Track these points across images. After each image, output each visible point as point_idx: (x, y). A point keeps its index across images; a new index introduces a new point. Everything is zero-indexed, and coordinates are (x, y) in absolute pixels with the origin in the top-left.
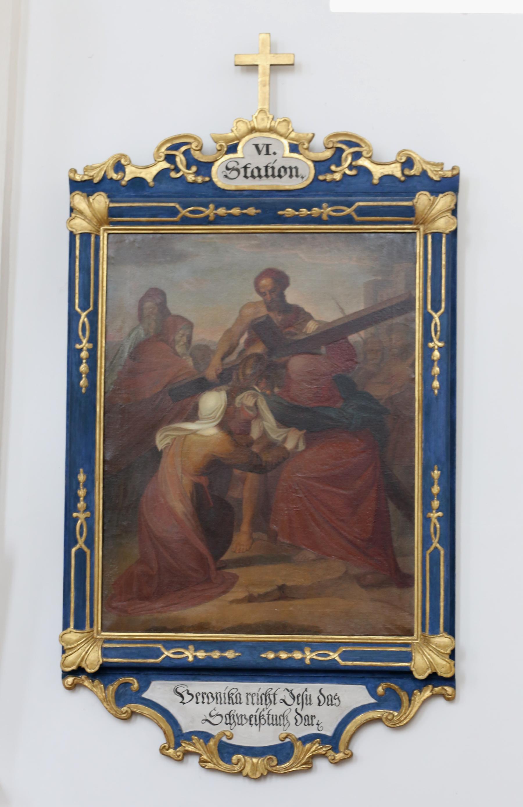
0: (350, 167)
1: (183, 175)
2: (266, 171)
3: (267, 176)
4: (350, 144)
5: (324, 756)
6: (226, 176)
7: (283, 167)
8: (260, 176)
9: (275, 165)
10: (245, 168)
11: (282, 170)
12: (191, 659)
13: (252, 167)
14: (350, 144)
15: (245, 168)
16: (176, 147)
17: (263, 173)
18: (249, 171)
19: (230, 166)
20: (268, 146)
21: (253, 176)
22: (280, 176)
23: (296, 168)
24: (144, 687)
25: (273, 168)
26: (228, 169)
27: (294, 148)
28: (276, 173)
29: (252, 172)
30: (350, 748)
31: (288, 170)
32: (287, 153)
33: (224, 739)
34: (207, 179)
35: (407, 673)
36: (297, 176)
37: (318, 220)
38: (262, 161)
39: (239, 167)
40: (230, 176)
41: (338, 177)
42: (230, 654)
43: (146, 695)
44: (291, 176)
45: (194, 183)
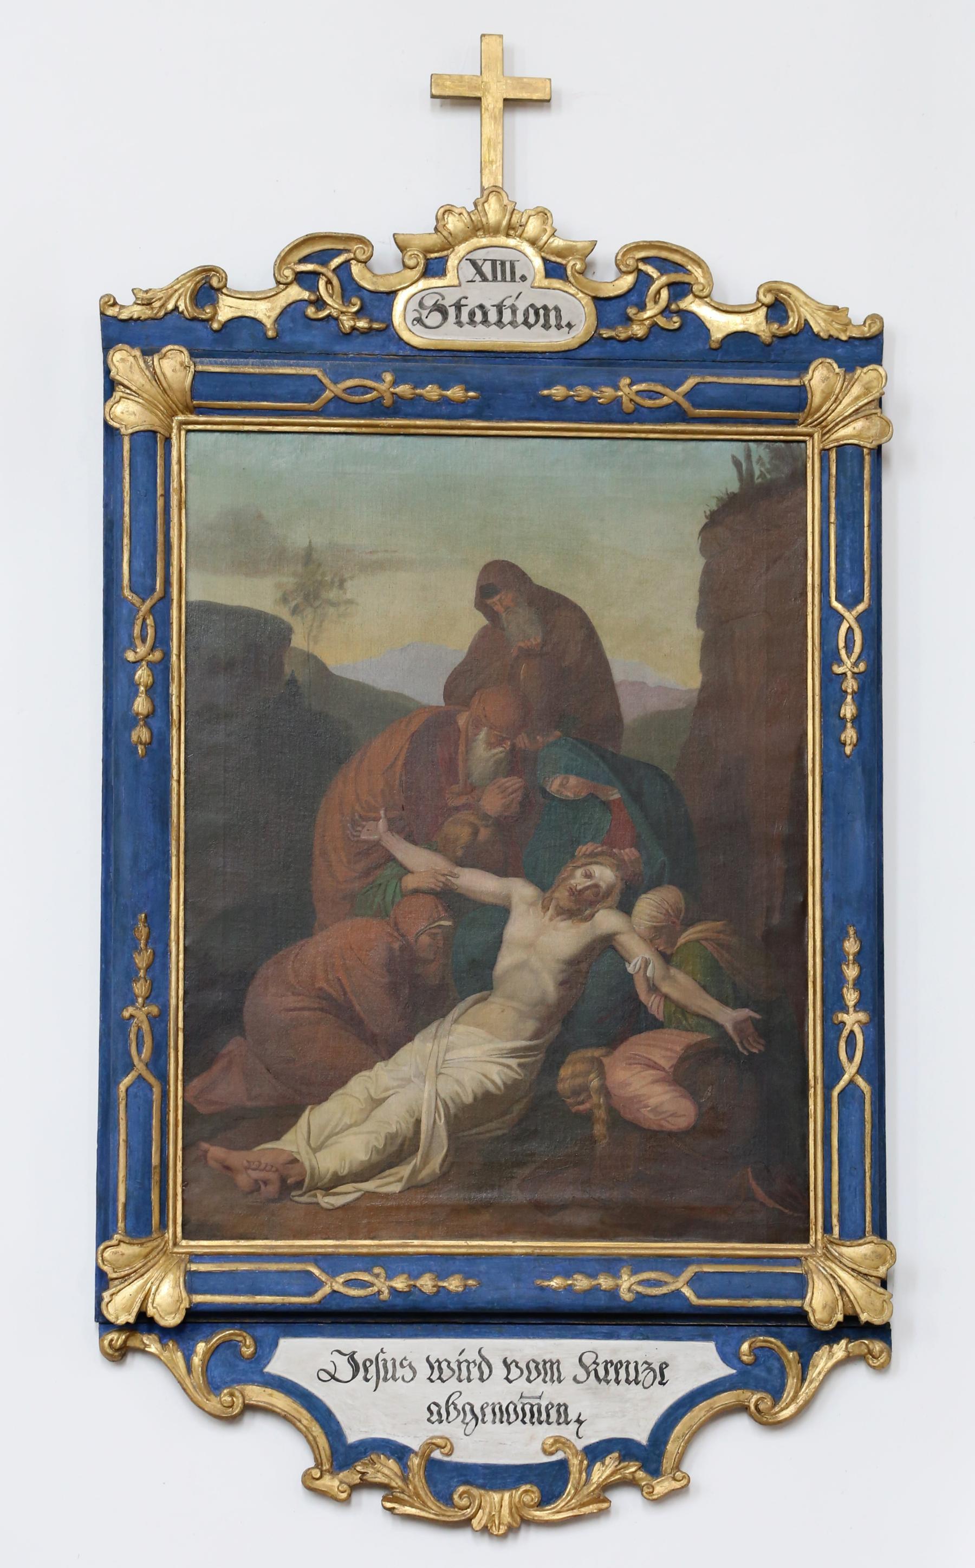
0: (666, 312)
2: (500, 313)
3: (499, 323)
4: (664, 265)
5: (630, 1483)
6: (419, 320)
7: (532, 306)
9: (517, 303)
10: (458, 307)
11: (531, 311)
12: (385, 1295)
13: (472, 303)
14: (664, 265)
15: (458, 307)
16: (323, 257)
17: (493, 316)
21: (472, 322)
23: (557, 309)
24: (265, 1351)
27: (554, 270)
28: (520, 318)
29: (472, 314)
30: (685, 1468)
31: (542, 312)
33: (437, 1455)
35: (800, 1316)
36: (559, 327)
40: (428, 322)
41: (638, 330)
42: (454, 1284)
43: (275, 1367)
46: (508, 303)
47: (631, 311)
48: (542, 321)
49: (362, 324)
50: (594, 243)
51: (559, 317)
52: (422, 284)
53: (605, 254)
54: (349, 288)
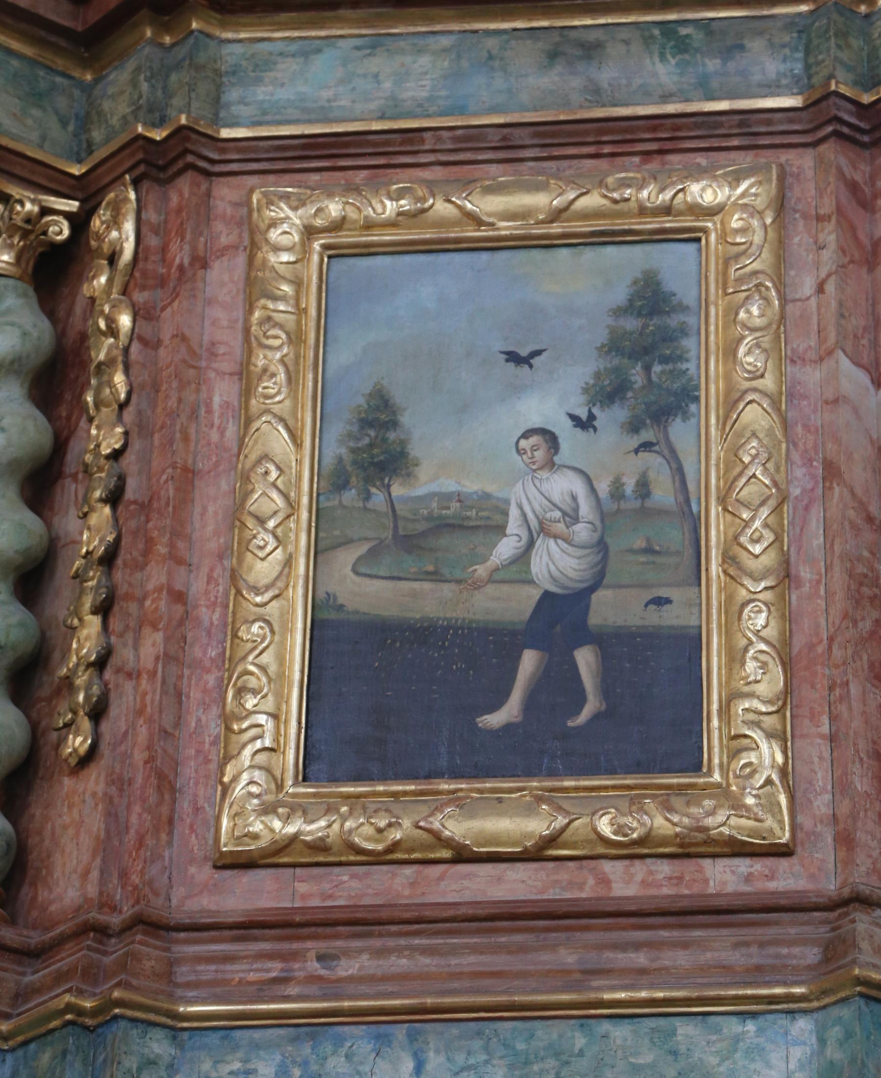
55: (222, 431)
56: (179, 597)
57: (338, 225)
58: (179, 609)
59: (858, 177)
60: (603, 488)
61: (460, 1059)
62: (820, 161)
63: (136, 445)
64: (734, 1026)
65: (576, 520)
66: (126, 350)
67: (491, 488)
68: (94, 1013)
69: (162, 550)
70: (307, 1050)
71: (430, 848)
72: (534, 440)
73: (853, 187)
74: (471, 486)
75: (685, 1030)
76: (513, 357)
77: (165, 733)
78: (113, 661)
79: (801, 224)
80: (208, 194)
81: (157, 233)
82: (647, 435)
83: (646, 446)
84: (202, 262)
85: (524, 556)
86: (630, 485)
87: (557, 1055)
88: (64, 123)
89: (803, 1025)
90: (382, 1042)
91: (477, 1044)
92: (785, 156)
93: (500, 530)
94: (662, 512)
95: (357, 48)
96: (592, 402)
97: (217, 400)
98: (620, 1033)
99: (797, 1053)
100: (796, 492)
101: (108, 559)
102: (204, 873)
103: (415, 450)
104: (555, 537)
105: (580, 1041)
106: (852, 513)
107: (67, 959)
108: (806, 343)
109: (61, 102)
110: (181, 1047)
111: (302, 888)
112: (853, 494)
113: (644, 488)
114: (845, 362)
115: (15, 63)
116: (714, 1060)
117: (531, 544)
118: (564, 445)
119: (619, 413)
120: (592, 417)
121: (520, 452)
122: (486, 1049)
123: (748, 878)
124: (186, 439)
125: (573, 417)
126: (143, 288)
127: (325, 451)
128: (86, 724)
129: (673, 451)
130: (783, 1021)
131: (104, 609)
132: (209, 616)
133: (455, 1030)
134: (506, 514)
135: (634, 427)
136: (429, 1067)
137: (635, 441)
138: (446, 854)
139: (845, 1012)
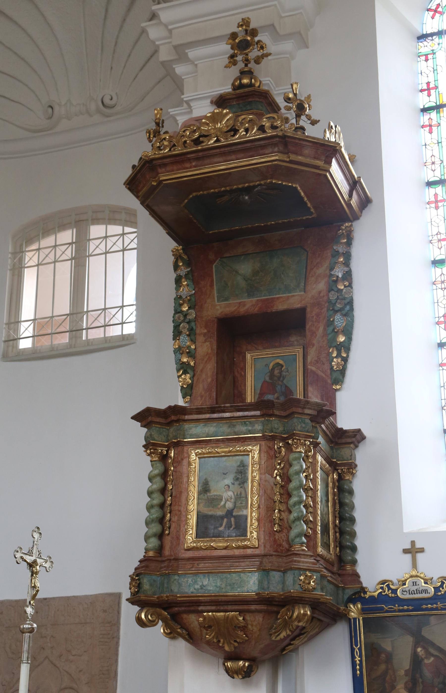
1: (386, 594)
3: (417, 593)
6: (403, 594)
8: (414, 594)
10: (409, 591)
17: (416, 592)
18: (410, 591)
19: (404, 590)
20: (416, 582)
21: (412, 594)
22: (421, 593)
25: (419, 590)
26: (403, 591)
27: (426, 583)
28: (420, 592)
29: (412, 592)
32: (423, 584)
34: (396, 595)
37: (437, 609)
38: (414, 588)
39: (406, 590)
44: (425, 593)
45: (392, 597)
46: (418, 589)
47: (441, 589)
48: (424, 592)
49: (393, 595)
50: (433, 578)
51: (427, 591)
52: (402, 587)
53: (435, 579)
54: (389, 588)
55: (185, 485)
56: (180, 511)
57: (200, 454)
58: (180, 513)
59: (270, 445)
60: (235, 494)
61: (214, 579)
62: (265, 443)
63: (174, 488)
64: (248, 574)
65: (232, 499)
66: (173, 473)
67: (221, 494)
68: (168, 573)
69: (177, 504)
70: (195, 577)
71: (211, 548)
72: (227, 486)
73: (269, 447)
74: (218, 494)
75: (242, 574)
76: (224, 474)
77: (178, 531)
78: (172, 520)
79: (262, 453)
80: (183, 449)
81: (177, 454)
82: (241, 486)
83: (241, 487)
84: (182, 459)
85: (225, 505)
86: (239, 493)
87: (226, 578)
88: (165, 436)
89: (257, 574)
90: (204, 576)
91: (216, 577)
92: (261, 442)
93: (222, 500)
94: (243, 497)
95: (203, 426)
96: (234, 481)
97: (185, 480)
98: (234, 575)
99: (256, 577)
100: (260, 494)
101: (171, 505)
102: (183, 551)
103: (211, 488)
104: (229, 501)
105: (229, 576)
106: (267, 498)
107: (166, 564)
108: (263, 471)
109: (164, 433)
110: (179, 577)
111: (196, 553)
112: (268, 495)
113: (241, 493)
114: (267, 475)
115: (157, 429)
116: (245, 579)
117: (226, 502)
118: (231, 488)
119: (238, 482)
120: (234, 483)
121: (225, 488)
122: (217, 577)
123: (253, 551)
124: (180, 487)
125: (232, 483)
126: (175, 463)
127: (199, 489)
128: (168, 530)
129: (245, 488)
130: (254, 573)
131: (170, 513)
132: (184, 513)
133: (213, 575)
134: (223, 498)
135: (239, 484)
136: (210, 580)
137: (240, 487)
138: (214, 549)
139: (261, 573)
